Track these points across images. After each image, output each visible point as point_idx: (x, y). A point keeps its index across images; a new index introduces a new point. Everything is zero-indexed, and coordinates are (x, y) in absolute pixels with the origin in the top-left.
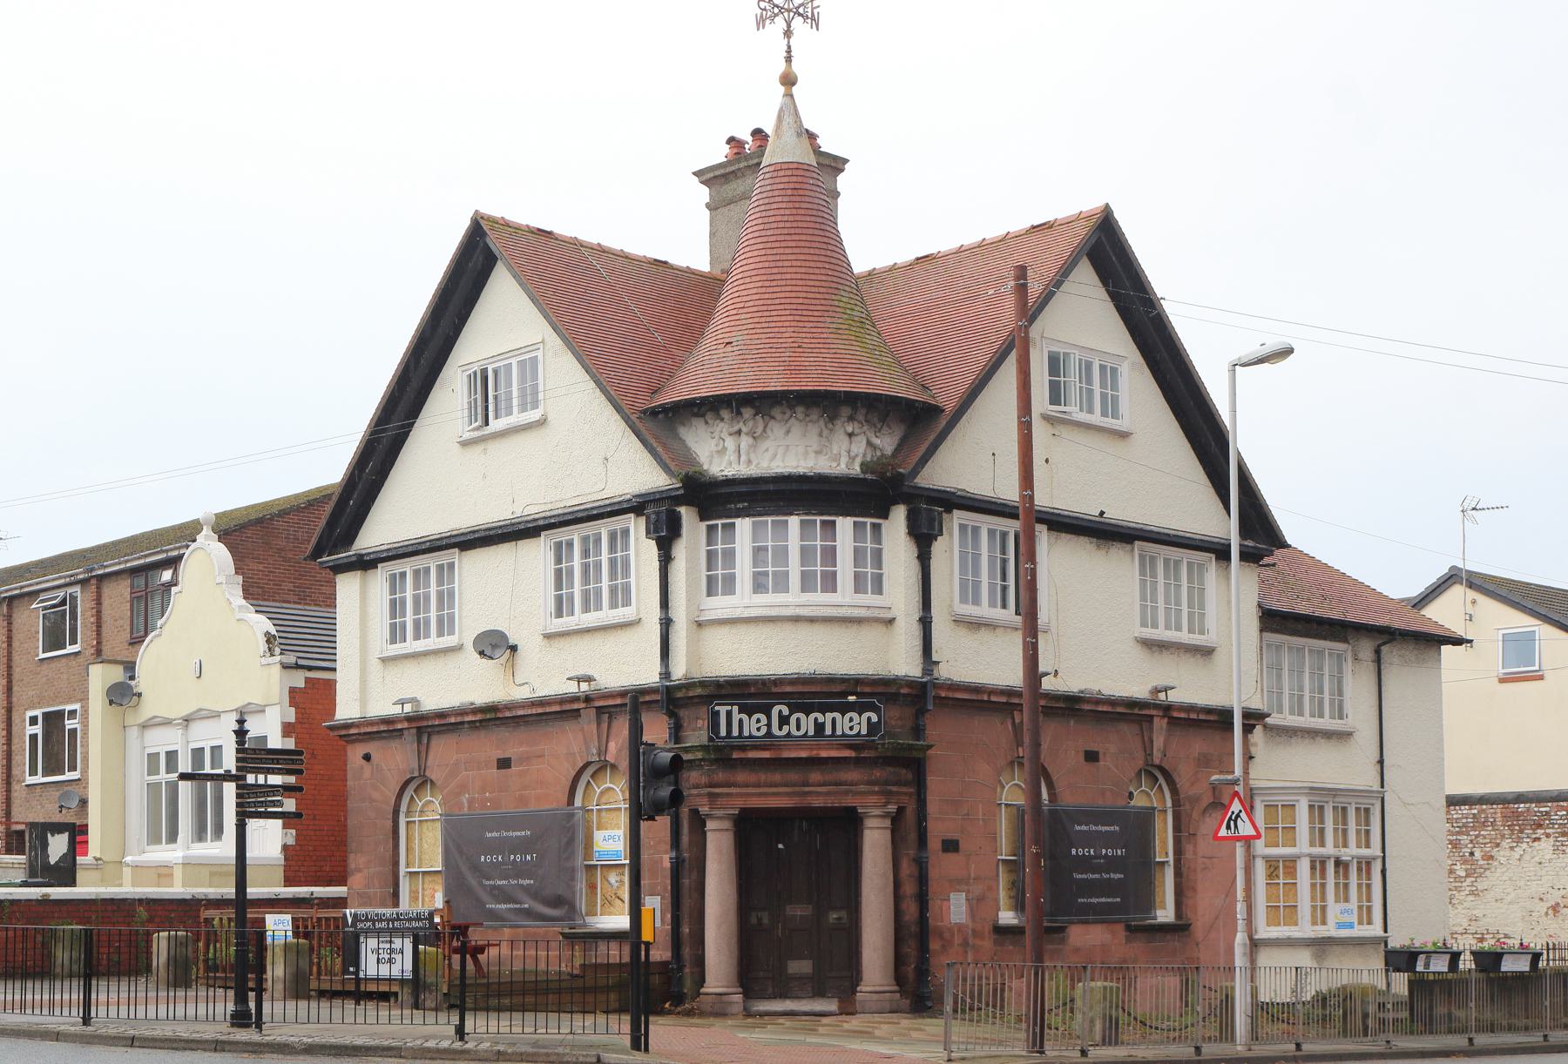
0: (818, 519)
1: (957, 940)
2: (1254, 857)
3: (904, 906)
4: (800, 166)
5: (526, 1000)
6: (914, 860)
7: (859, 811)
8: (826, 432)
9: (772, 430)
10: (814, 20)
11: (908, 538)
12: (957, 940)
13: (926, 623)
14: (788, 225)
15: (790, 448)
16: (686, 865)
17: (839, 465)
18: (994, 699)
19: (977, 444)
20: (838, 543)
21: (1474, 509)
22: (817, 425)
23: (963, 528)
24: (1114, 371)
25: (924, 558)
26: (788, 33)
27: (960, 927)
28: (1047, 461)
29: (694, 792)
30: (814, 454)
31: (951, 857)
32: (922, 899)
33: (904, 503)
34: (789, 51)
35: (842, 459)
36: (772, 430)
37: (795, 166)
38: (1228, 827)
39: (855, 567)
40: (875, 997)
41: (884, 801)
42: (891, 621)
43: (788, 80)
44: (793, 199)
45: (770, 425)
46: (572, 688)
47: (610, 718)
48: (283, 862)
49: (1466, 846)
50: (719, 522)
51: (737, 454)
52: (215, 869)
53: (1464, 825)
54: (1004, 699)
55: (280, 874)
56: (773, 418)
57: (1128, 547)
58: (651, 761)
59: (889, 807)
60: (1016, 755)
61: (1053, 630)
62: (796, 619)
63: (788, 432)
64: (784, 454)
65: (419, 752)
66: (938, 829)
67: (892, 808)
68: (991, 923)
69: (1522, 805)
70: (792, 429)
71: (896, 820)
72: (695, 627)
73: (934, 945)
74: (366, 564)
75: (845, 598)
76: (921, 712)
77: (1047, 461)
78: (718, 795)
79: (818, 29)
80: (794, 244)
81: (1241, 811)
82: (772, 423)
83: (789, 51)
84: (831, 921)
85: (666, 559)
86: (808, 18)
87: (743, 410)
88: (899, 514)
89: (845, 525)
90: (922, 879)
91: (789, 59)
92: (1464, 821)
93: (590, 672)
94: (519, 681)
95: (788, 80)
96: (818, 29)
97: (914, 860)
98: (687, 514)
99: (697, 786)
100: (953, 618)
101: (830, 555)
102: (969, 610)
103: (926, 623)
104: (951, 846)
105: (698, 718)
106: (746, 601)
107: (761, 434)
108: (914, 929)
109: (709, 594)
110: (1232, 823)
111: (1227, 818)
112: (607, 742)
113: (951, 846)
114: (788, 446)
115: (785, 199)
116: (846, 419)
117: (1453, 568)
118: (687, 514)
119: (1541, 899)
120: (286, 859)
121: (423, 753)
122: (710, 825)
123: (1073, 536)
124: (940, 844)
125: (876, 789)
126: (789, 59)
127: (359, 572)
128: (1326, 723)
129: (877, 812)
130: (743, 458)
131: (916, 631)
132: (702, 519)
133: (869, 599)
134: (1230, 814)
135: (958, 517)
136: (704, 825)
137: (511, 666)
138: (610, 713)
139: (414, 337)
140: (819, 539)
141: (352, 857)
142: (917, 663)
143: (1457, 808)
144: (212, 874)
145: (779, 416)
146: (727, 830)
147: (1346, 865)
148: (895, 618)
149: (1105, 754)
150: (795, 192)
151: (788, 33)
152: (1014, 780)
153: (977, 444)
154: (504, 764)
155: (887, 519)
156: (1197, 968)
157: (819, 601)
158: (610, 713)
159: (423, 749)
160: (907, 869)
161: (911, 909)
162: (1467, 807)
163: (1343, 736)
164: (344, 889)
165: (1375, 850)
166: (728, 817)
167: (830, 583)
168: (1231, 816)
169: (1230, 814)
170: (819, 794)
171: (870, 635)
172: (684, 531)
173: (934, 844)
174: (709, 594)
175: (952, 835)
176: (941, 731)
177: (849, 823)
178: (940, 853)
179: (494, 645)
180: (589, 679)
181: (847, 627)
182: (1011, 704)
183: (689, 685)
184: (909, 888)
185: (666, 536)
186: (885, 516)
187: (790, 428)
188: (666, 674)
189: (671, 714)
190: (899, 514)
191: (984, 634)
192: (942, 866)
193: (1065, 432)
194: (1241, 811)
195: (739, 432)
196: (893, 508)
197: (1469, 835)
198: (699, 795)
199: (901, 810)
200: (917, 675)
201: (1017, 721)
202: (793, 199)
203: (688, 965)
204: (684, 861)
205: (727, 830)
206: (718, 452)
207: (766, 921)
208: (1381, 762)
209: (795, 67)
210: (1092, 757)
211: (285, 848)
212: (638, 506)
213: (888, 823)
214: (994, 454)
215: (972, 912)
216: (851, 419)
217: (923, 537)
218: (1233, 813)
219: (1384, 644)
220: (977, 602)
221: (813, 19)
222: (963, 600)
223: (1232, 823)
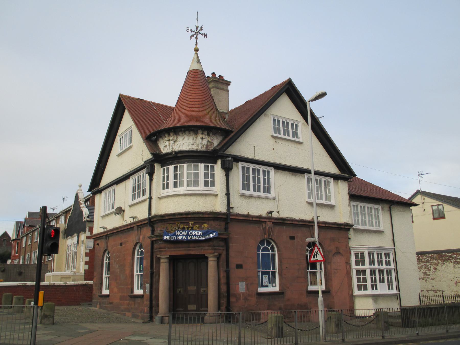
0: (193, 164)
1: (242, 298)
2: (352, 269)
3: (222, 287)
4: (197, 70)
5: (25, 327)
6: (225, 271)
7: (206, 255)
8: (195, 138)
9: (179, 139)
11: (222, 169)
12: (242, 298)
13: (228, 194)
14: (191, 85)
15: (184, 143)
16: (154, 274)
17: (199, 148)
18: (254, 219)
19: (248, 143)
20: (199, 172)
21: (421, 174)
22: (192, 136)
23: (243, 168)
24: (296, 125)
25: (227, 176)
27: (243, 293)
28: (273, 149)
29: (156, 250)
30: (191, 145)
31: (240, 270)
32: (228, 284)
33: (220, 159)
34: (197, 42)
35: (200, 146)
36: (179, 139)
37: (196, 70)
38: (314, 257)
39: (205, 179)
40: (211, 317)
41: (213, 252)
42: (217, 195)
43: (196, 50)
44: (194, 78)
45: (178, 138)
46: (132, 221)
47: (141, 229)
48: (84, 274)
49: (429, 266)
51: (169, 146)
52: (62, 276)
53: (428, 260)
55: (83, 277)
56: (180, 135)
57: (303, 175)
58: (47, 232)
59: (215, 254)
60: (264, 237)
61: (277, 199)
62: (185, 195)
63: (184, 139)
64: (183, 145)
65: (106, 242)
66: (234, 261)
67: (216, 254)
68: (256, 292)
69: (443, 254)
70: (185, 138)
71: (218, 258)
72: (158, 199)
73: (232, 299)
75: (201, 188)
76: (227, 223)
77: (273, 149)
78: (162, 251)
79: (206, 38)
80: (193, 90)
81: (318, 251)
82: (179, 137)
83: (197, 42)
84: (202, 291)
85: (151, 179)
86: (203, 35)
87: (170, 133)
88: (219, 162)
89: (201, 166)
90: (228, 278)
91: (196, 44)
92: (428, 258)
93: (136, 216)
94: (125, 220)
95: (196, 50)
96: (206, 38)
97: (225, 271)
98: (157, 166)
99: (157, 249)
100: (240, 194)
101: (196, 175)
102: (246, 192)
103: (228, 194)
104: (239, 266)
105: (158, 227)
106: (172, 190)
107: (176, 140)
108: (225, 294)
109: (164, 189)
110: (315, 255)
111: (314, 254)
112: (140, 236)
113: (239, 266)
114: (183, 143)
115: (192, 78)
116: (200, 134)
118: (157, 166)
119: (452, 280)
120: (85, 273)
121: (107, 243)
122: (162, 261)
123: (283, 171)
124: (235, 266)
125: (211, 248)
126: (196, 44)
127: (99, 194)
128: (374, 228)
129: (211, 255)
130: (171, 147)
131: (225, 198)
132: (162, 167)
133: (210, 188)
134: (314, 252)
135: (241, 164)
136: (160, 261)
137: (123, 216)
138: (140, 227)
139: (107, 131)
140: (193, 170)
142: (225, 208)
143: (425, 255)
144: (61, 278)
145: (181, 135)
146: (166, 262)
147: (383, 271)
148: (218, 194)
149: (297, 237)
150: (195, 77)
152: (265, 245)
153: (248, 143)
154: (121, 244)
155: (216, 164)
156: (310, 311)
157: (193, 189)
158: (140, 227)
159: (107, 241)
160: (223, 274)
161: (224, 288)
162: (428, 255)
163: (381, 232)
164: (93, 282)
166: (166, 258)
167: (196, 183)
168: (315, 253)
169: (314, 252)
170: (193, 250)
171: (210, 200)
172: (156, 171)
173: (232, 265)
174: (164, 189)
175: (239, 263)
176: (234, 229)
177: (204, 258)
178: (235, 269)
179: (120, 211)
180: (136, 218)
181: (202, 197)
182: (253, 220)
183: (155, 216)
184: (223, 281)
186: (215, 163)
187: (184, 138)
189: (150, 226)
190: (219, 162)
192: (235, 273)
193: (278, 141)
195: (169, 140)
196: (218, 160)
197: (429, 262)
198: (157, 251)
199: (220, 255)
200: (225, 212)
201: (264, 226)
202: (194, 78)
203: (154, 307)
204: (154, 272)
205: (166, 262)
206: (165, 147)
207: (182, 292)
208: (393, 240)
209: (198, 47)
211: (85, 270)
213: (215, 259)
214: (254, 146)
215: (247, 288)
216: (202, 134)
217: (227, 169)
218: (315, 252)
220: (249, 189)
221: (205, 35)
222: (244, 189)
223: (315, 255)
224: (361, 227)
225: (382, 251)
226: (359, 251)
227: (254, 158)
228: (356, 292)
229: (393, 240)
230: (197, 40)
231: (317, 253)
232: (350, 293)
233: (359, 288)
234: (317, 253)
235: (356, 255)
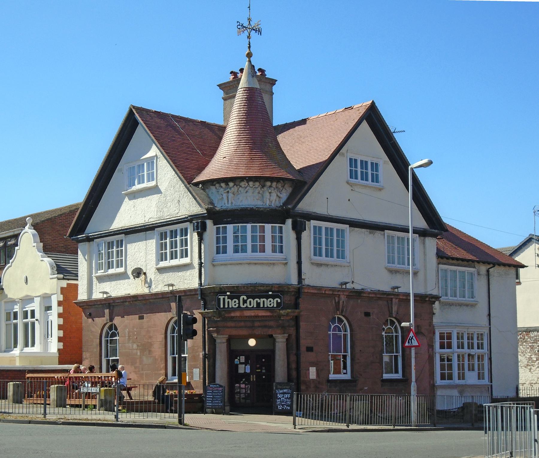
1: (312, 385)
2: (435, 353)
10: (259, 31)
12: (312, 385)
13: (299, 263)
24: (377, 164)
26: (249, 37)
28: (349, 200)
31: (310, 353)
32: (298, 369)
34: (249, 42)
38: (409, 342)
46: (166, 289)
48: (58, 355)
49: (536, 348)
50: (221, 226)
53: (536, 340)
54: (331, 293)
57: (382, 232)
66: (304, 342)
81: (413, 336)
86: (257, 31)
88: (289, 222)
89: (268, 227)
90: (298, 363)
91: (249, 47)
92: (535, 338)
97: (295, 354)
102: (317, 259)
103: (299, 263)
104: (310, 349)
113: (310, 349)
120: (59, 354)
124: (306, 349)
126: (249, 47)
135: (313, 223)
141: (84, 353)
143: (533, 332)
147: (473, 356)
149: (372, 313)
151: (249, 37)
160: (293, 358)
162: (536, 332)
165: (485, 350)
168: (410, 338)
173: (303, 349)
180: (172, 285)
184: (294, 366)
185: (201, 230)
186: (284, 223)
188: (201, 284)
190: (289, 222)
191: (323, 268)
192: (305, 357)
194: (413, 336)
197: (537, 343)
199: (290, 336)
210: (367, 314)
211: (59, 350)
212: (190, 219)
214: (327, 198)
218: (410, 337)
219: (491, 268)
222: (315, 255)
224: (451, 299)
226: (446, 330)
227: (327, 214)
228: (438, 381)
231: (412, 338)
232: (432, 382)
233: (443, 377)
234: (412, 338)
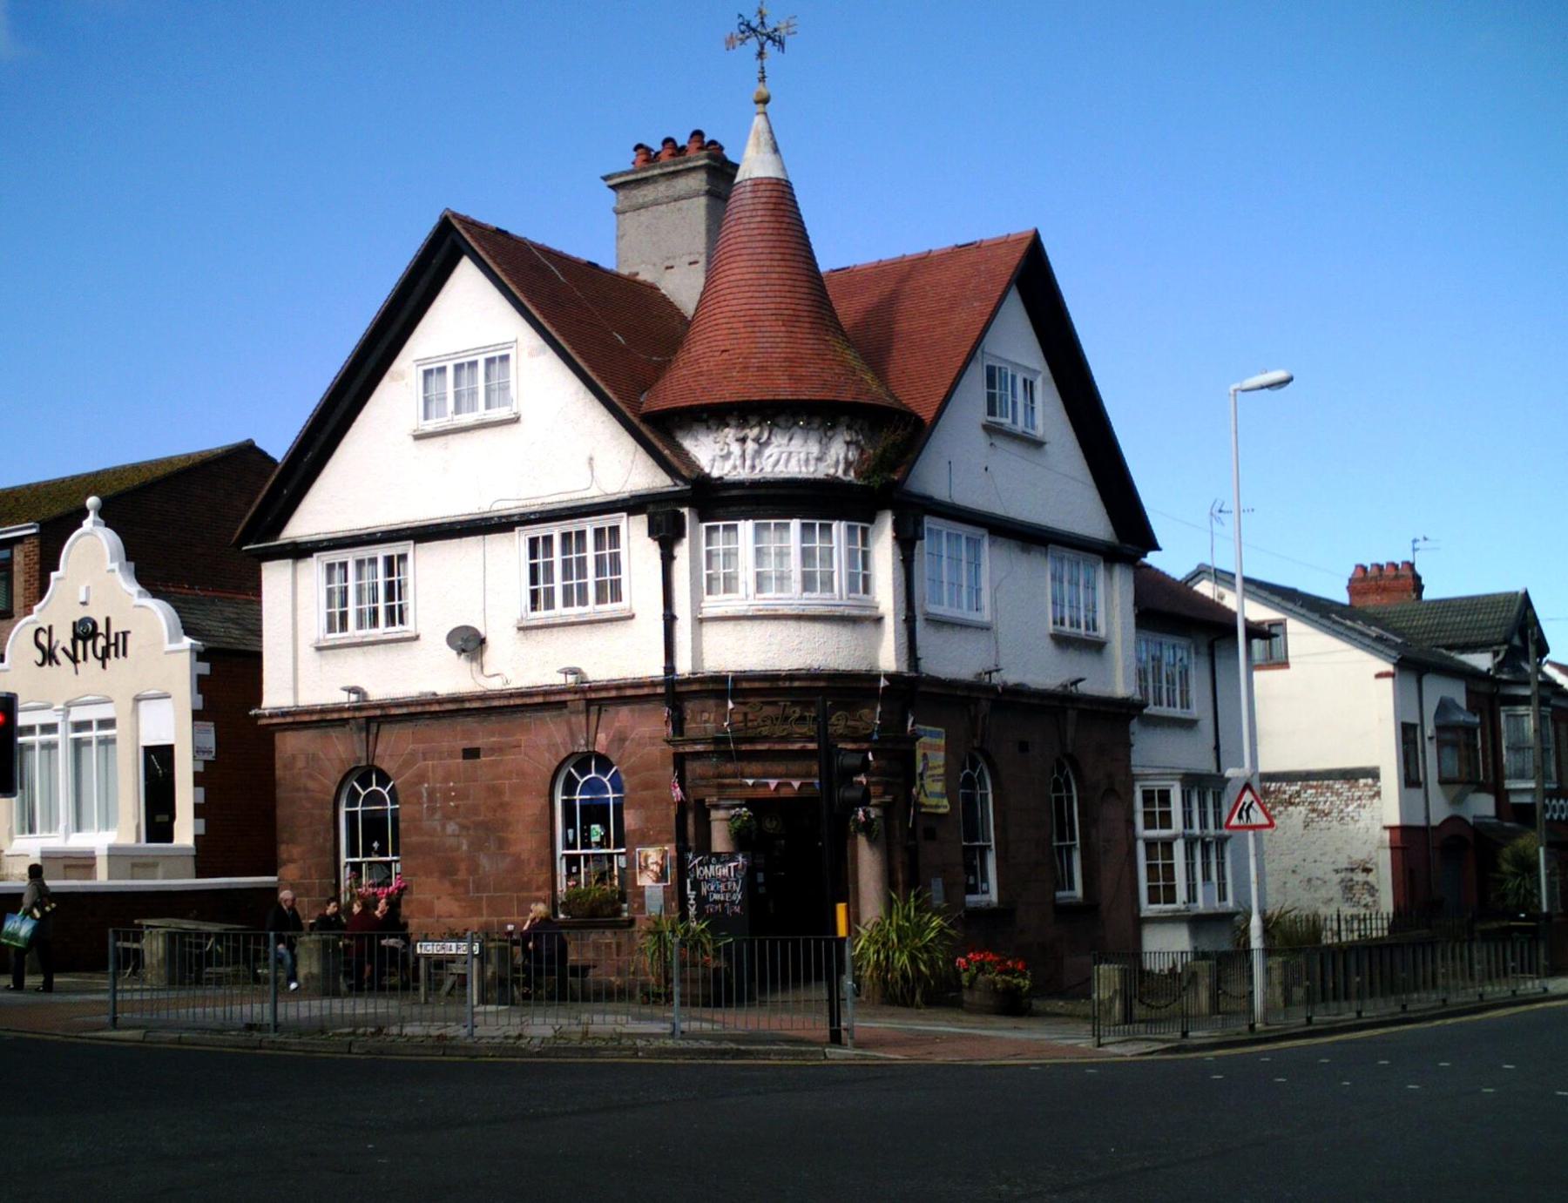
10: (780, 43)
21: (1220, 511)
24: (1031, 383)
26: (761, 55)
28: (986, 469)
34: (763, 68)
38: (1240, 817)
46: (559, 680)
48: (194, 853)
50: (721, 523)
54: (965, 693)
57: (1043, 549)
63: (790, 439)
69: (1273, 785)
74: (300, 551)
77: (986, 469)
89: (839, 528)
105: (703, 711)
110: (1244, 814)
112: (596, 733)
117: (1201, 565)
119: (1294, 872)
122: (715, 814)
128: (1177, 712)
130: (748, 463)
132: (702, 520)
136: (709, 815)
141: (283, 847)
144: (134, 865)
151: (761, 55)
154: (471, 754)
163: (1189, 724)
164: (274, 879)
185: (667, 535)
186: (871, 520)
188: (670, 667)
191: (946, 633)
194: (1252, 802)
196: (879, 513)
206: (722, 457)
208: (1217, 748)
210: (1024, 747)
211: (197, 837)
212: (633, 505)
218: (1244, 804)
223: (1244, 814)
224: (1164, 710)
225: (1171, 783)
226: (1157, 785)
227: (948, 500)
229: (1217, 748)
230: (762, 63)
231: (1250, 805)
234: (1250, 805)
235: (1148, 797)
